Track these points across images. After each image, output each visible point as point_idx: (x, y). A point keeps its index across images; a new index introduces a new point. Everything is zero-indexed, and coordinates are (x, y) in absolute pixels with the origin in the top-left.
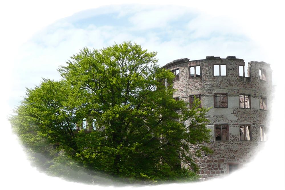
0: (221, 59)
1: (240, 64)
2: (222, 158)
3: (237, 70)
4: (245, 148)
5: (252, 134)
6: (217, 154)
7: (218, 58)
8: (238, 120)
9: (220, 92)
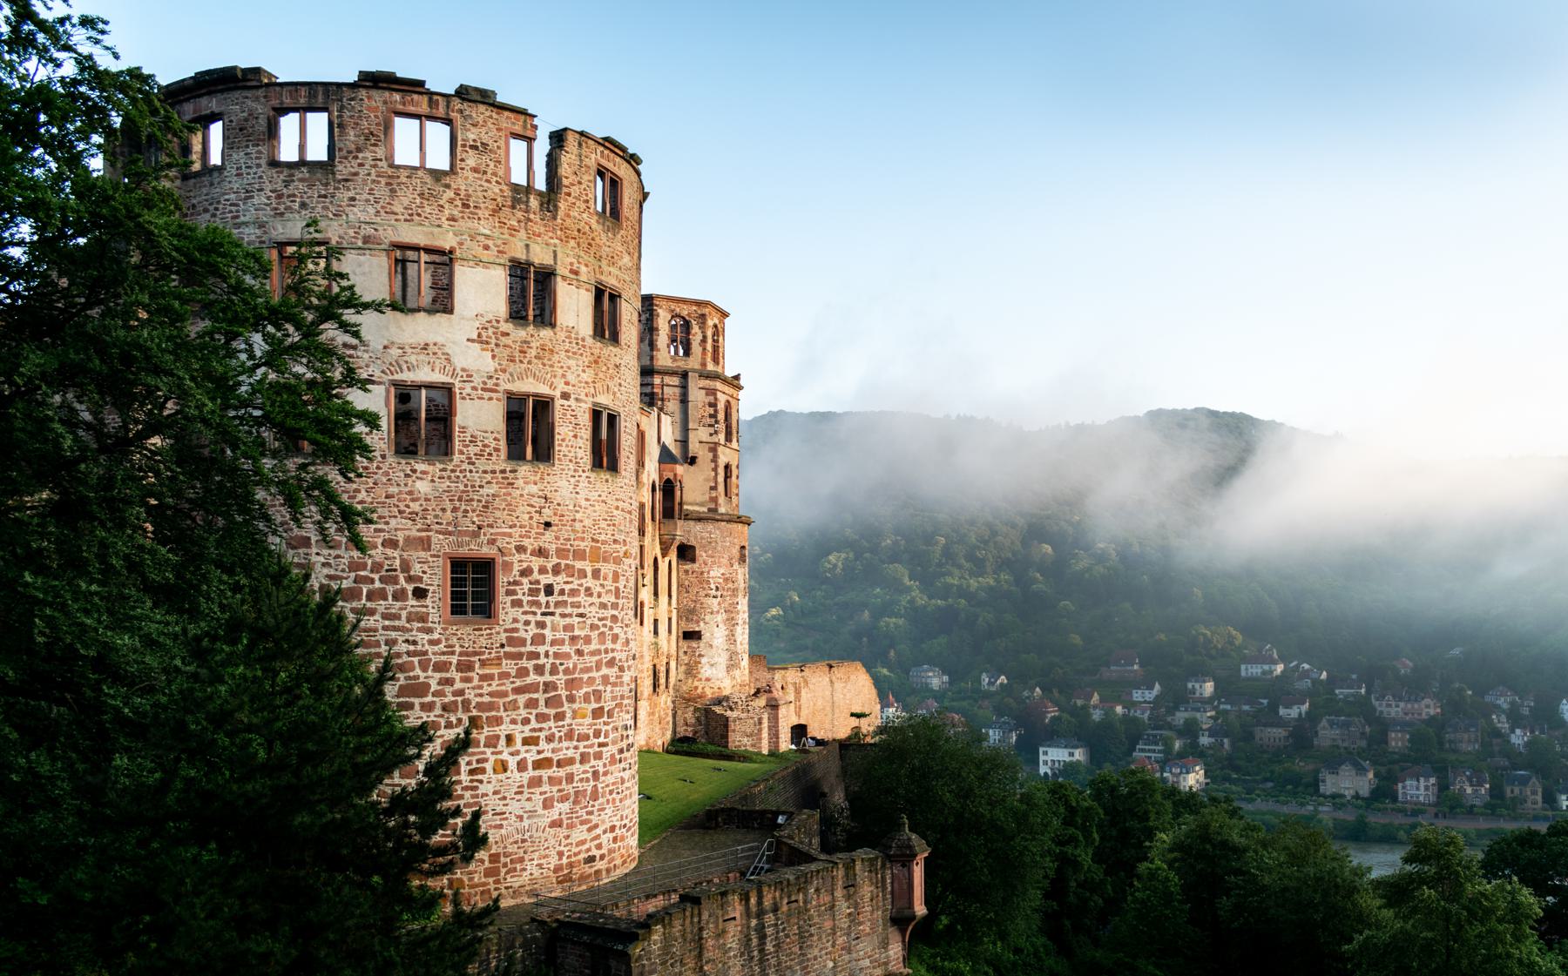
0: (431, 94)
1: (518, 129)
2: (418, 530)
3: (502, 152)
4: (525, 492)
5: (557, 437)
6: (400, 512)
7: (414, 86)
8: (496, 371)
9: (422, 240)
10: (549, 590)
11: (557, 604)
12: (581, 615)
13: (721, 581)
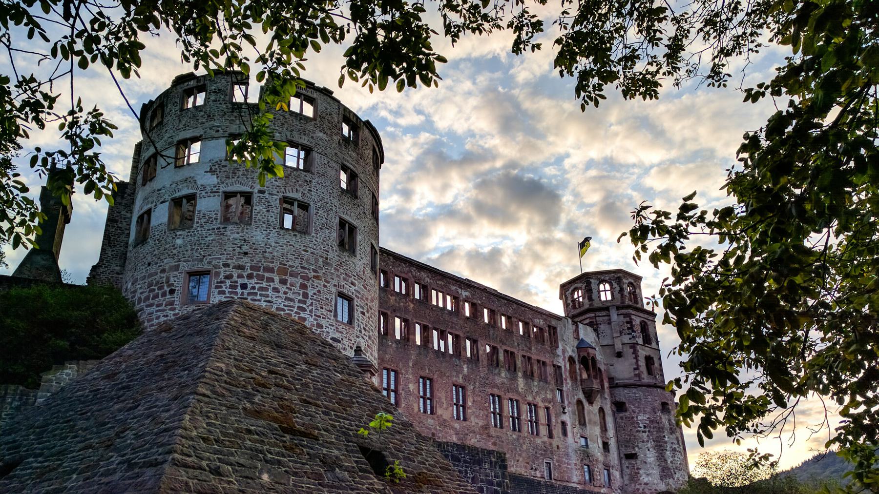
6: (169, 255)
10: (244, 286)
11: (249, 294)
12: (269, 302)
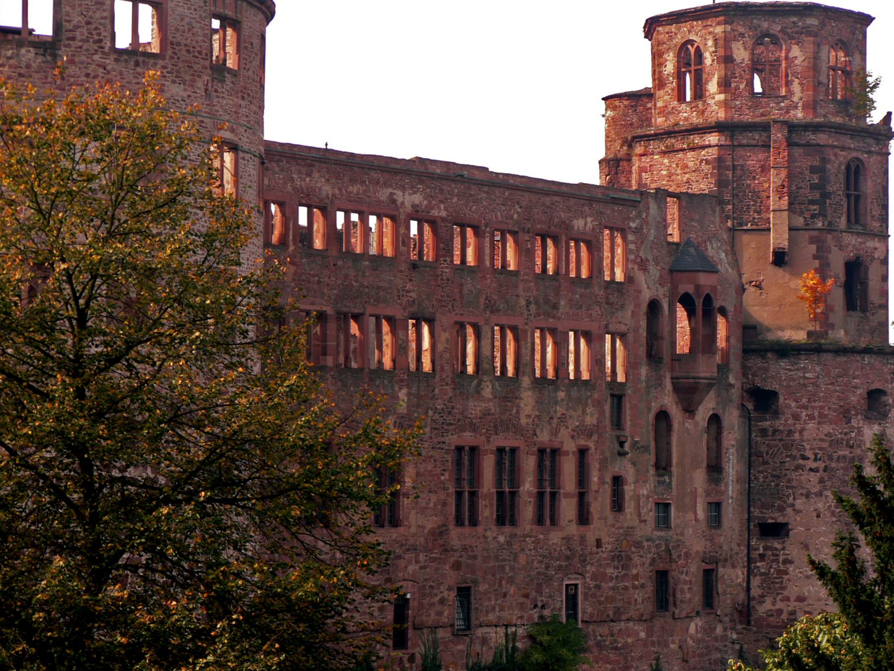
13: (825, 445)
